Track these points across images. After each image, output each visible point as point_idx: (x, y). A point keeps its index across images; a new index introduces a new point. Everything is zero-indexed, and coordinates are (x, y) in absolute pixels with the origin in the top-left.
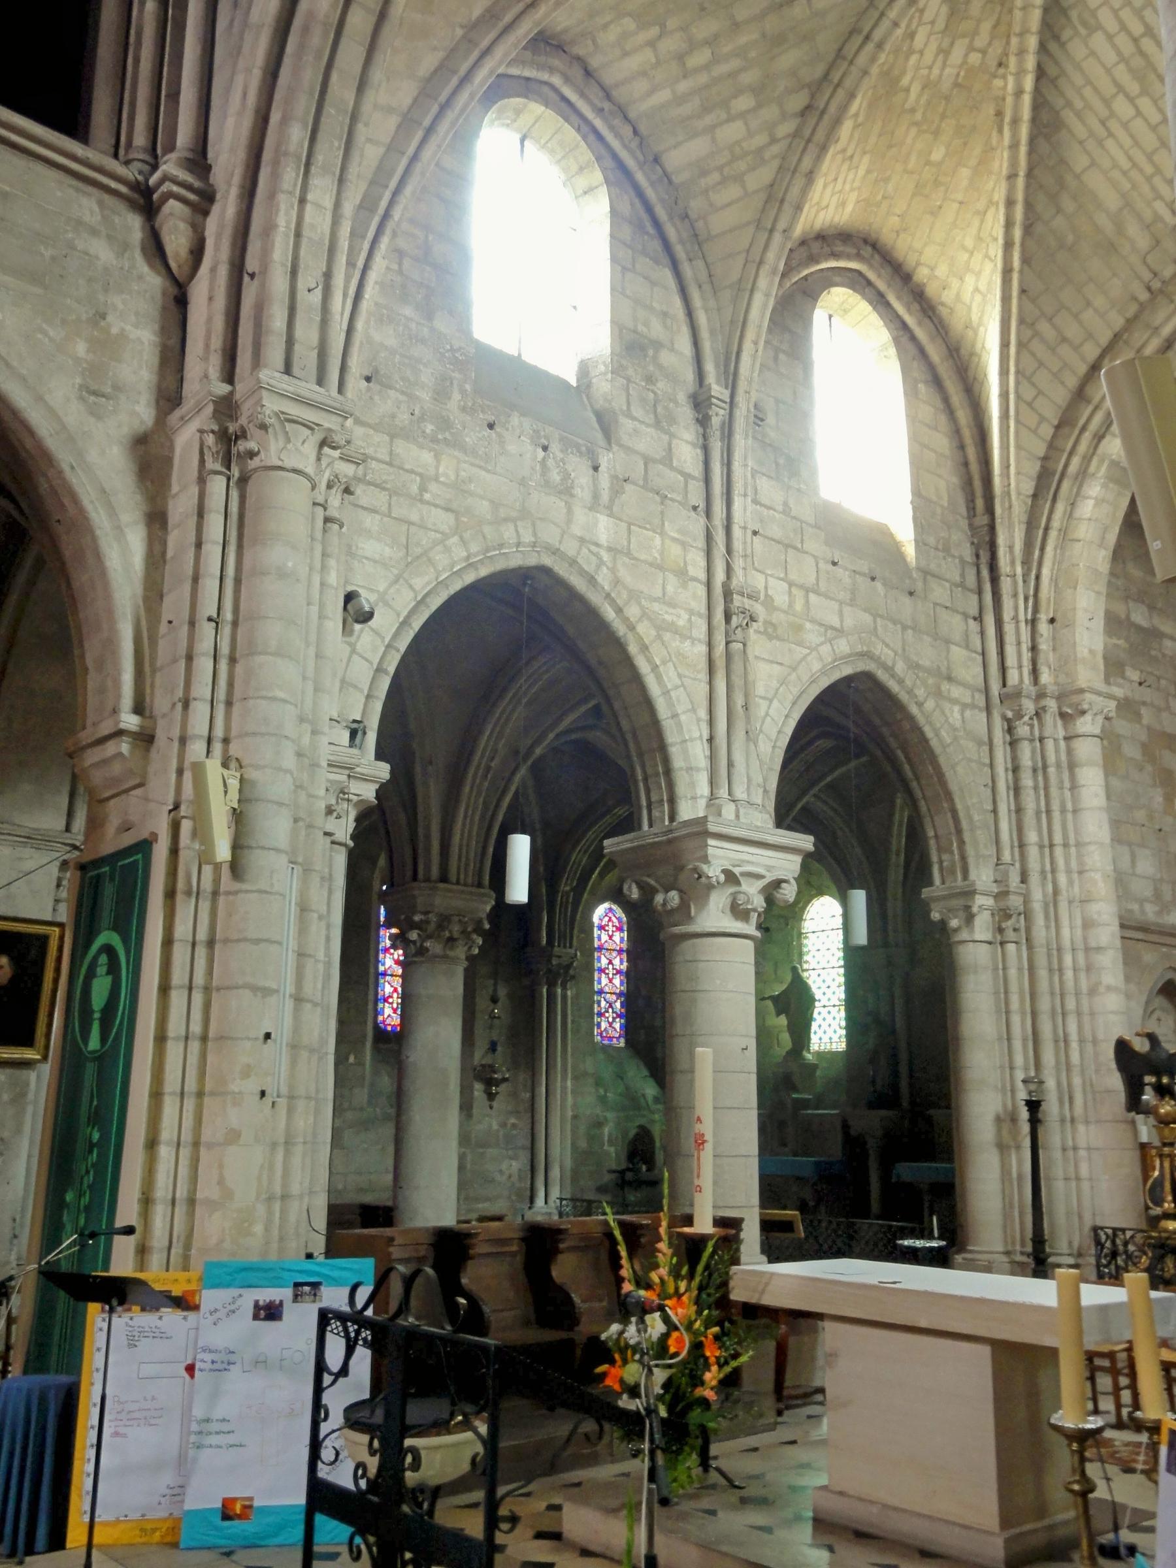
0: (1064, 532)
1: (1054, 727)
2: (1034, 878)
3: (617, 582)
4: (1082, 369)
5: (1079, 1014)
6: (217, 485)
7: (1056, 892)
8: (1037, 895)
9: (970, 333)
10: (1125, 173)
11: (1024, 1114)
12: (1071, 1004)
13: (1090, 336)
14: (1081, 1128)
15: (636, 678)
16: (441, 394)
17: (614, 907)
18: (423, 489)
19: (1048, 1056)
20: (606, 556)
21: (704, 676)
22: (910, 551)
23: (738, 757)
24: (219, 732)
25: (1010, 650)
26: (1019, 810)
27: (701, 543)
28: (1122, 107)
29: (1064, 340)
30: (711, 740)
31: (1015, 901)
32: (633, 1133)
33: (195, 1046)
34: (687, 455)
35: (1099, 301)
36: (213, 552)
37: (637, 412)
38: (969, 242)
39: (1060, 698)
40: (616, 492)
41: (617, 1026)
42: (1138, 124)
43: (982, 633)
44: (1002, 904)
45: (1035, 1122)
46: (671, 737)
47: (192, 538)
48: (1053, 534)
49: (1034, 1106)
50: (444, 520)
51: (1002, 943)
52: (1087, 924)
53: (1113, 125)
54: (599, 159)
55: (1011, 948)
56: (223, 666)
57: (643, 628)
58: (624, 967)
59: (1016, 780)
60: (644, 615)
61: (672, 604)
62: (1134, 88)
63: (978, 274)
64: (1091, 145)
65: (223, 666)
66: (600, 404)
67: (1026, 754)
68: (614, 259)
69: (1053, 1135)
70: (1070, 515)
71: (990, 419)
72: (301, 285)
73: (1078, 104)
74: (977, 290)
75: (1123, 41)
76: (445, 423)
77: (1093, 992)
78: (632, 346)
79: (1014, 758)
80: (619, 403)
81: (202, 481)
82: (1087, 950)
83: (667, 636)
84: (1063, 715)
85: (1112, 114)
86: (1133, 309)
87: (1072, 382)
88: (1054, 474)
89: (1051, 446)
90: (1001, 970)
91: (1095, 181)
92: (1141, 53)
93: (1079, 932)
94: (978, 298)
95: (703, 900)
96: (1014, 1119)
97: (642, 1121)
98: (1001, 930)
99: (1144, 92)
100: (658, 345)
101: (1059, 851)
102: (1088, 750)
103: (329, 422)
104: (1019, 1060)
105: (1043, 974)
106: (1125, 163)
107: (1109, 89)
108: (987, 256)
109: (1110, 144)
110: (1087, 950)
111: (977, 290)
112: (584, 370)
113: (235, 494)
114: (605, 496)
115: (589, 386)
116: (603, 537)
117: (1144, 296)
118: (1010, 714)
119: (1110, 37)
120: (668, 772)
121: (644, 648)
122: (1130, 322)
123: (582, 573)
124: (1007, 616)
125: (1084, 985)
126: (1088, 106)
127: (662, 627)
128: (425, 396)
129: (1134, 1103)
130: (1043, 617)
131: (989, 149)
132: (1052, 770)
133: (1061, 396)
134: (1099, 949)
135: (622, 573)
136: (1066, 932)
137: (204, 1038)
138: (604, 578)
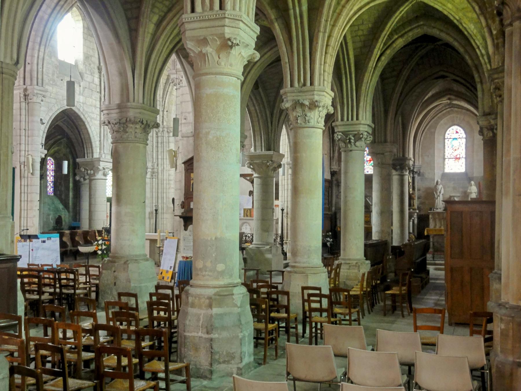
0: (171, 92)
2: (159, 165)
3: (84, 110)
5: (166, 193)
6: (23, 104)
8: (160, 169)
11: (154, 212)
12: (165, 191)
14: (165, 214)
15: (86, 129)
16: (53, 75)
17: (51, 158)
18: (51, 95)
19: (160, 201)
20: (82, 105)
21: (99, 128)
23: (105, 144)
24: (27, 150)
26: (158, 151)
27: (99, 99)
30: (100, 141)
31: (156, 170)
32: (57, 217)
33: (26, 202)
34: (97, 81)
36: (23, 117)
37: (88, 72)
39: (167, 128)
40: (84, 91)
41: (51, 190)
45: (156, 213)
46: (93, 141)
47: (19, 113)
48: (169, 93)
49: (156, 210)
50: (54, 101)
52: (169, 175)
54: (81, 14)
55: (154, 179)
56: (27, 138)
57: (88, 119)
58: (53, 175)
59: (157, 145)
60: (89, 116)
61: (93, 113)
65: (27, 138)
66: (80, 71)
67: (160, 140)
68: (84, 38)
69: (159, 216)
72: (39, 67)
76: (54, 81)
77: (169, 188)
78: (87, 57)
79: (157, 140)
80: (84, 71)
81: (20, 103)
82: (169, 180)
83: (93, 120)
84: (168, 132)
93: (167, 177)
95: (98, 173)
96: (152, 213)
97: (59, 214)
98: (152, 176)
100: (91, 56)
101: (165, 160)
103: (44, 93)
104: (154, 202)
105: (160, 185)
110: (169, 180)
112: (76, 62)
113: (27, 106)
114: (82, 92)
115: (78, 66)
116: (81, 101)
120: (92, 147)
121: (88, 123)
123: (78, 108)
125: (168, 188)
127: (92, 118)
128: (50, 75)
130: (165, 110)
135: (85, 108)
136: (165, 177)
137: (27, 201)
138: (81, 110)
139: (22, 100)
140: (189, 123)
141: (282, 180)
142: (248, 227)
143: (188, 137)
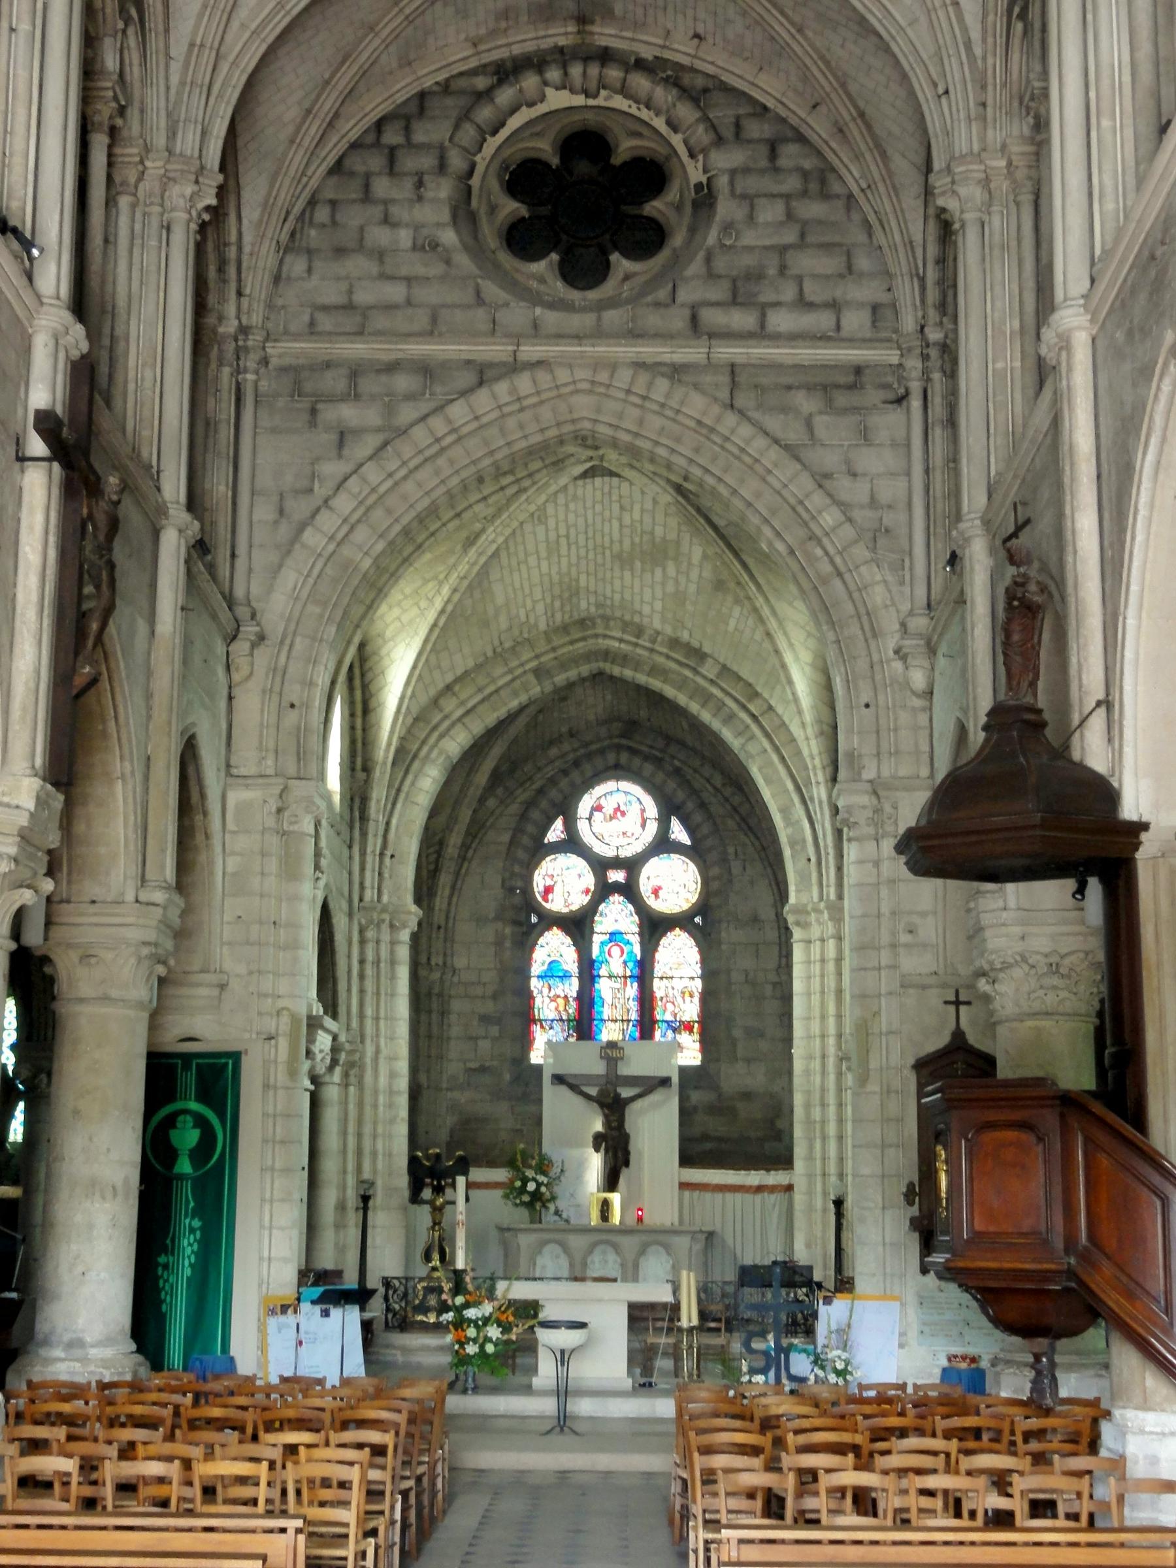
0: (407, 794)
1: (386, 936)
2: (368, 1041)
4: (441, 686)
7: (378, 1052)
9: (380, 641)
10: (514, 590)
12: (380, 1130)
13: (453, 667)
22: (337, 799)
25: (368, 874)
26: (362, 991)
28: (532, 560)
29: (439, 667)
35: (466, 650)
38: (408, 591)
42: (535, 572)
43: (351, 858)
44: (351, 1058)
48: (402, 796)
49: (365, 1199)
51: (347, 1085)
52: (393, 1075)
53: (523, 567)
55: (352, 1089)
62: (543, 554)
63: (405, 611)
64: (506, 572)
70: (413, 784)
71: (381, 705)
73: (512, 550)
74: (399, 619)
75: (552, 535)
77: (392, 1121)
79: (362, 952)
84: (392, 926)
85: (526, 562)
86: (481, 659)
87: (432, 692)
88: (408, 753)
89: (409, 731)
90: (344, 1103)
91: (497, 589)
92: (558, 542)
94: (397, 624)
99: (548, 558)
102: (404, 953)
105: (368, 1110)
106: (517, 585)
107: (531, 547)
108: (417, 604)
109: (516, 576)
111: (399, 619)
117: (490, 654)
118: (363, 921)
119: (547, 530)
122: (478, 667)
124: (369, 850)
126: (516, 554)
129: (415, 1198)
130: (388, 853)
131: (451, 552)
132: (382, 965)
133: (423, 699)
134: (399, 1093)
139: (271, 822)
140: (924, 946)
141: (808, 1106)
142: (612, 1257)
143: (924, 987)
